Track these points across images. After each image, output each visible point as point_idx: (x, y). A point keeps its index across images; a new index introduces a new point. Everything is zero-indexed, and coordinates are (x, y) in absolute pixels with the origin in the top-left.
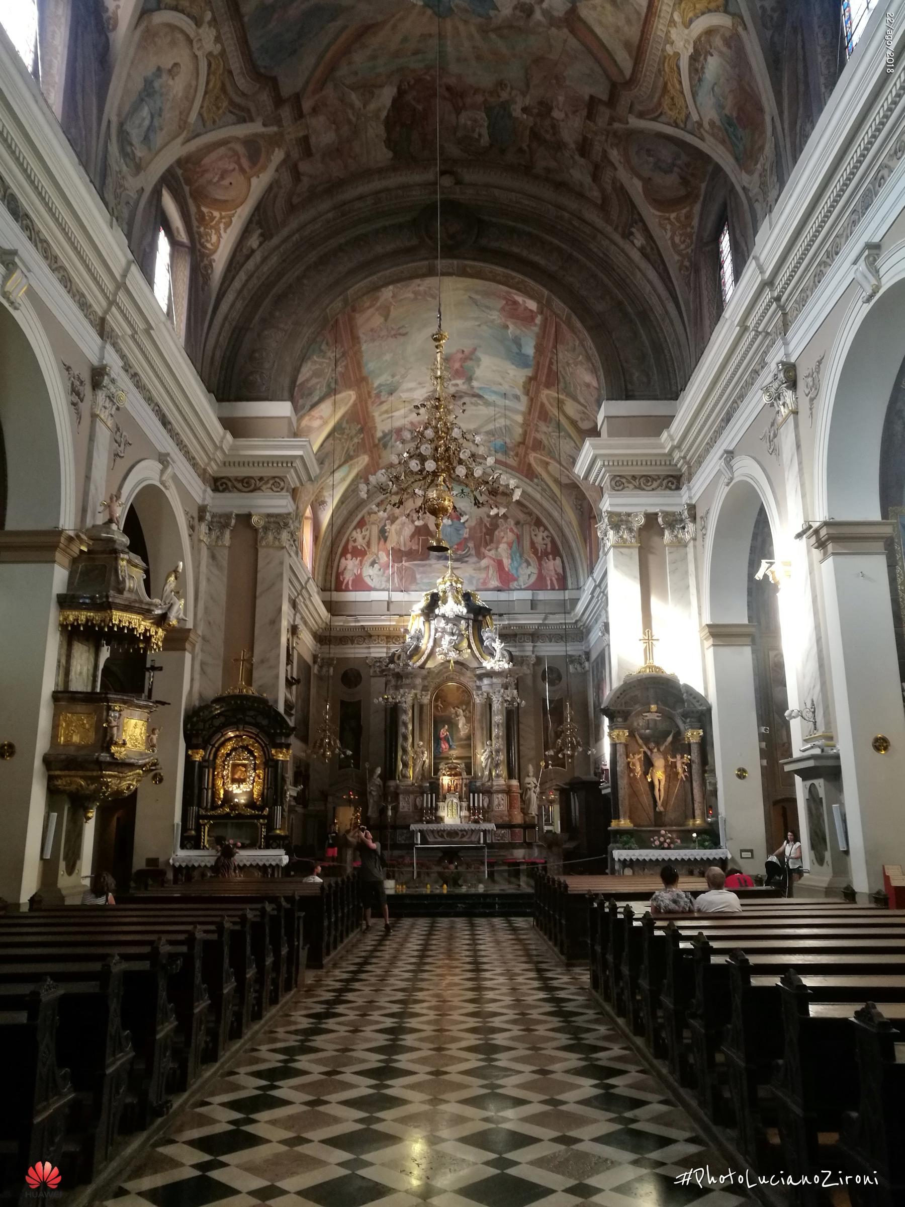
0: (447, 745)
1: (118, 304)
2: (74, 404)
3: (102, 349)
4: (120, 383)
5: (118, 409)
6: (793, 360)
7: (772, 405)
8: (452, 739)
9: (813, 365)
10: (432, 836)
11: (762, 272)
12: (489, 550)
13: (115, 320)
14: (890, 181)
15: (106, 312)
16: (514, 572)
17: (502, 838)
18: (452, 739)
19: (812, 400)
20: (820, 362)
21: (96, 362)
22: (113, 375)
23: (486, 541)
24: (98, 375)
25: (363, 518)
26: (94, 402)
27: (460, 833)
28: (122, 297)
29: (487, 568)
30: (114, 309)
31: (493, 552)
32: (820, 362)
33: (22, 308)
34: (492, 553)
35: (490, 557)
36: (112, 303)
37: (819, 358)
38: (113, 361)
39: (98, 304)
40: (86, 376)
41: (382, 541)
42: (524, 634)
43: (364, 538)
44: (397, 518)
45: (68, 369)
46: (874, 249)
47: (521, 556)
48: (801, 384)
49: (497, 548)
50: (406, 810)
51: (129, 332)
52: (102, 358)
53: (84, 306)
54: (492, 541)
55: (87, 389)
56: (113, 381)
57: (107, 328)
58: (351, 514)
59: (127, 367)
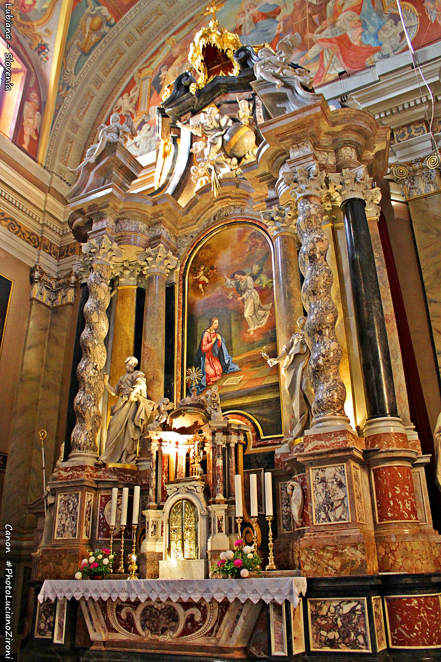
0: (218, 366)
8: (229, 344)
10: (100, 624)
12: (320, 32)
16: (371, 42)
17: (345, 635)
18: (229, 344)
23: (312, 22)
25: (133, 78)
27: (183, 615)
29: (321, 55)
31: (327, 31)
34: (327, 33)
35: (323, 40)
41: (155, 92)
42: (408, 126)
43: (131, 102)
44: (177, 57)
47: (380, 15)
49: (333, 25)
50: (68, 536)
54: (323, 18)
58: (117, 82)
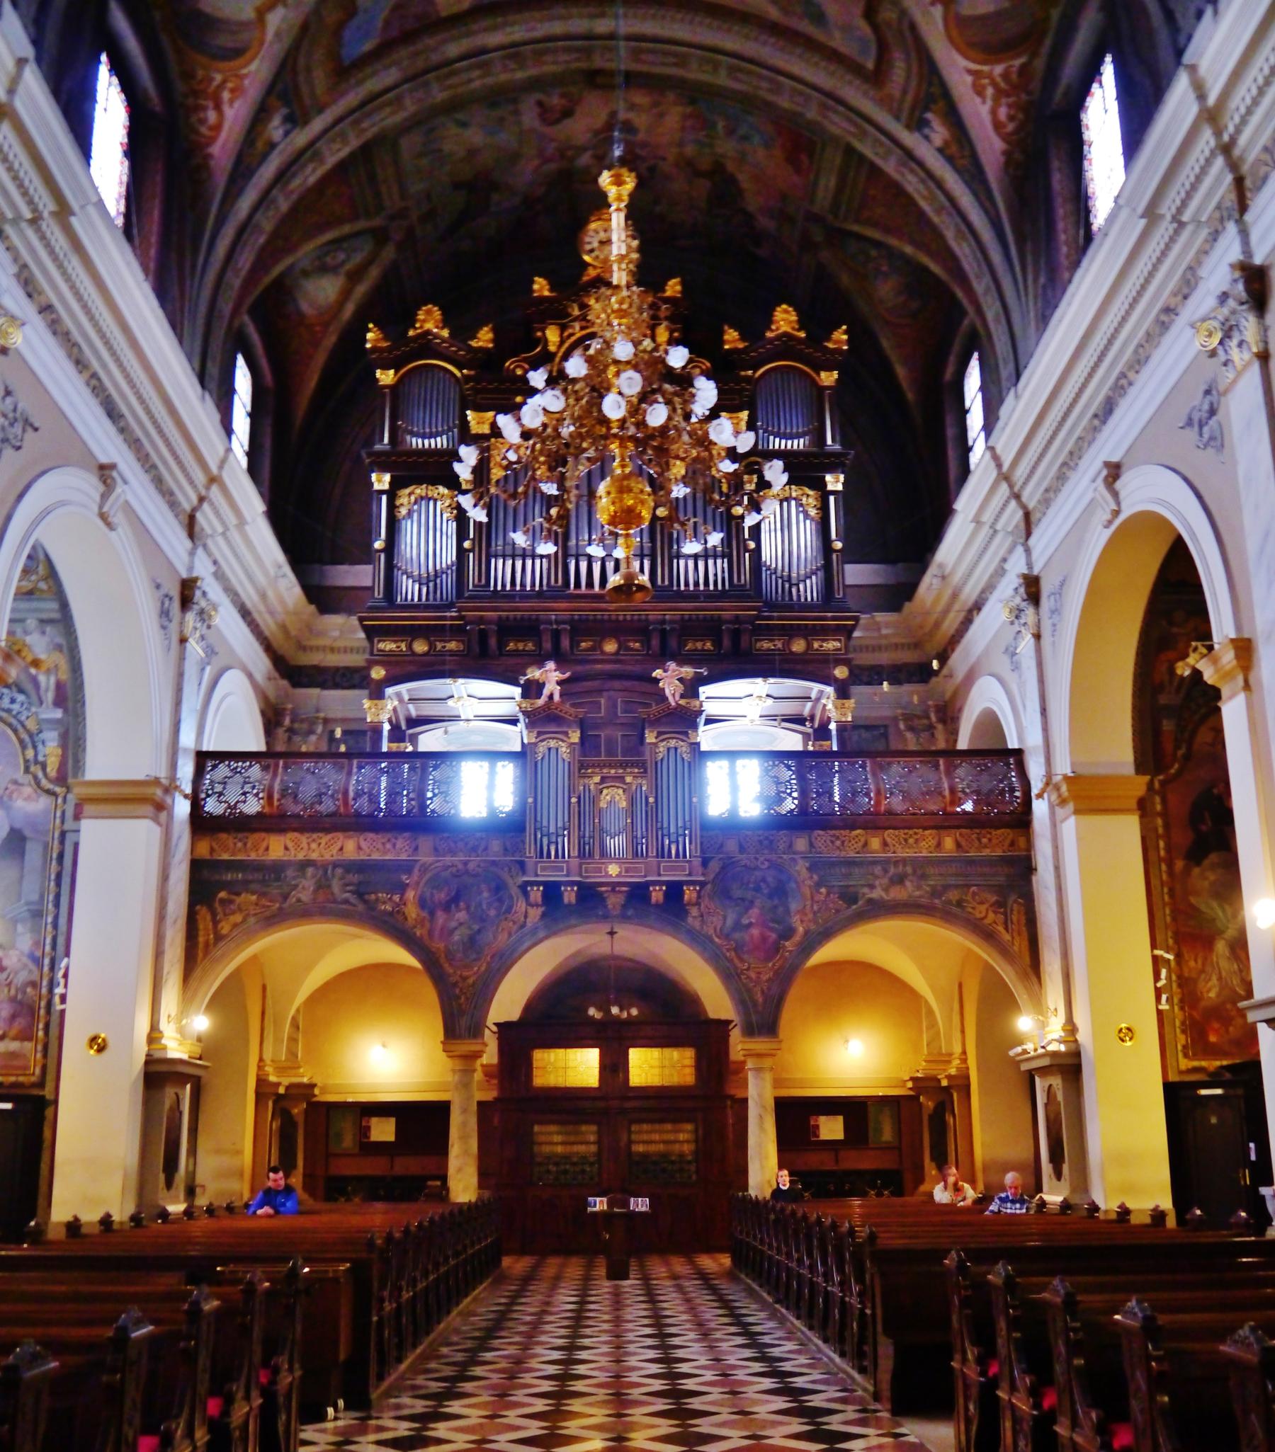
1: (212, 504)
2: (164, 628)
3: (192, 553)
4: (211, 595)
5: (209, 627)
6: (1036, 572)
7: (1012, 623)
9: (1057, 583)
11: (999, 465)
13: (205, 519)
14: (1132, 392)
15: (194, 510)
19: (1054, 625)
20: (1062, 584)
21: (185, 575)
22: (207, 589)
24: (187, 591)
26: (182, 623)
28: (215, 491)
30: (206, 506)
32: (1062, 584)
33: (120, 529)
36: (202, 499)
37: (1061, 578)
38: (203, 569)
39: (187, 499)
40: (175, 592)
45: (158, 587)
46: (1114, 472)
48: (1046, 603)
51: (220, 530)
52: (191, 568)
53: (173, 504)
55: (176, 605)
56: (204, 594)
57: (197, 529)
59: (219, 575)
